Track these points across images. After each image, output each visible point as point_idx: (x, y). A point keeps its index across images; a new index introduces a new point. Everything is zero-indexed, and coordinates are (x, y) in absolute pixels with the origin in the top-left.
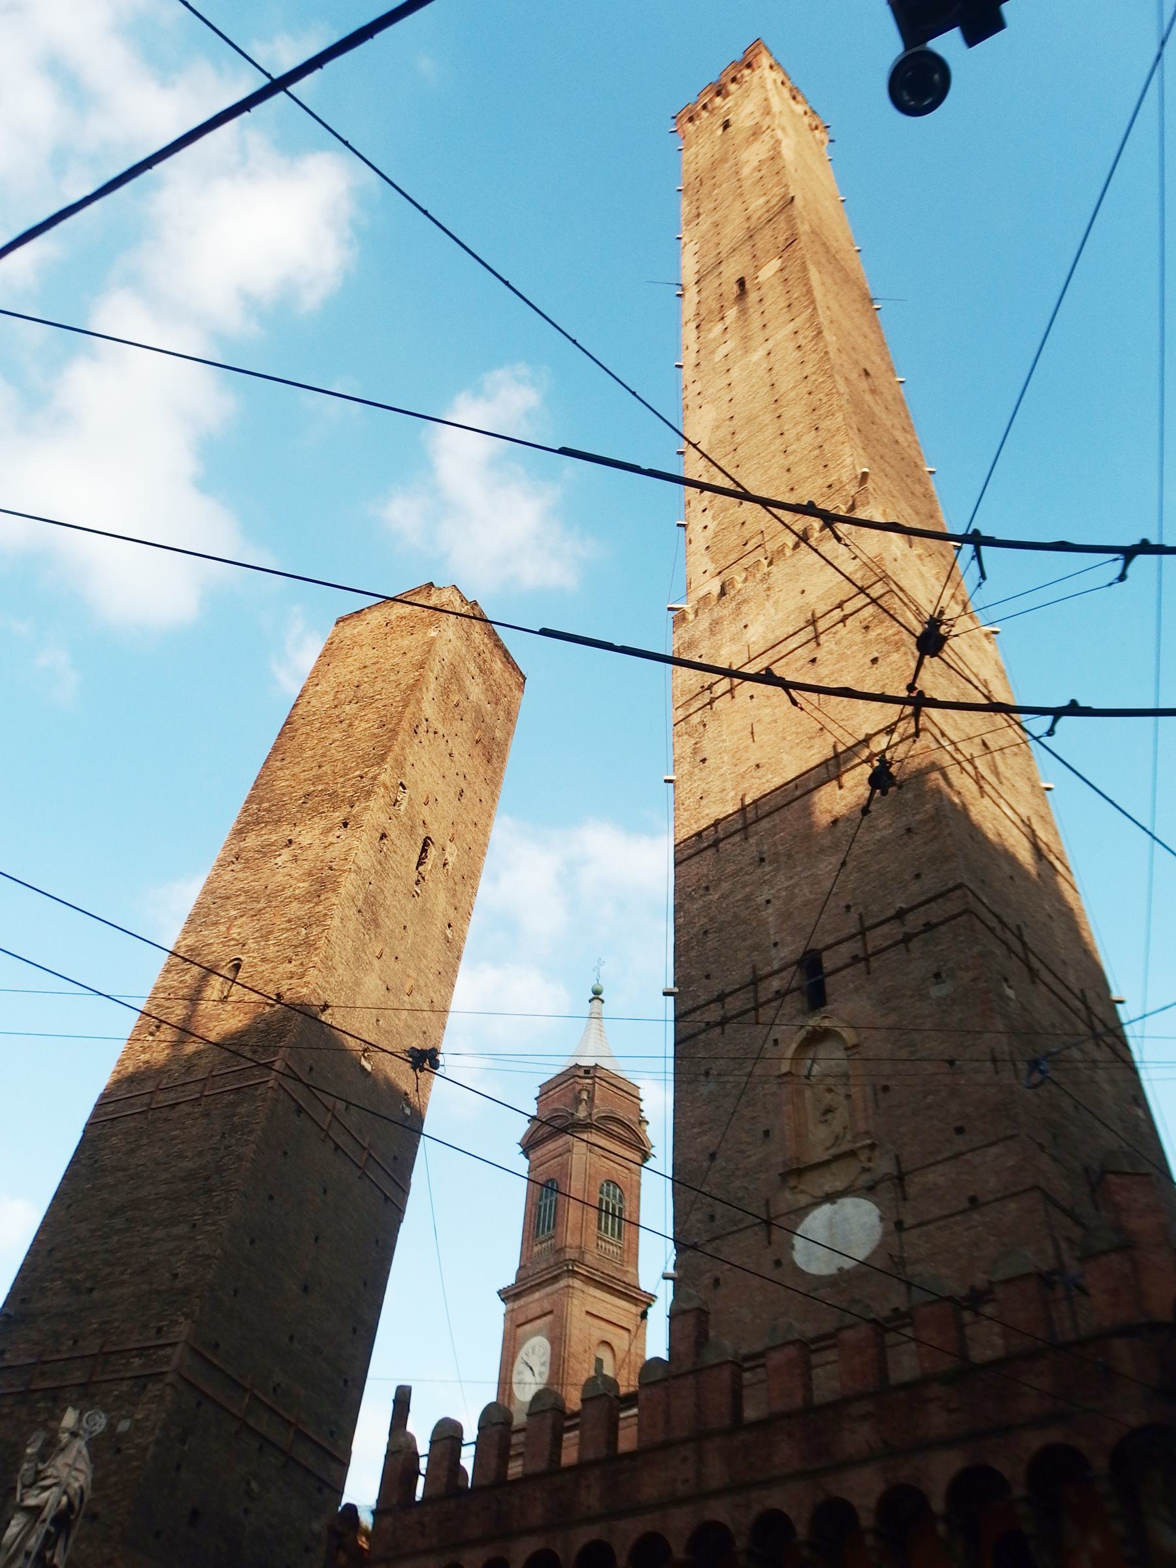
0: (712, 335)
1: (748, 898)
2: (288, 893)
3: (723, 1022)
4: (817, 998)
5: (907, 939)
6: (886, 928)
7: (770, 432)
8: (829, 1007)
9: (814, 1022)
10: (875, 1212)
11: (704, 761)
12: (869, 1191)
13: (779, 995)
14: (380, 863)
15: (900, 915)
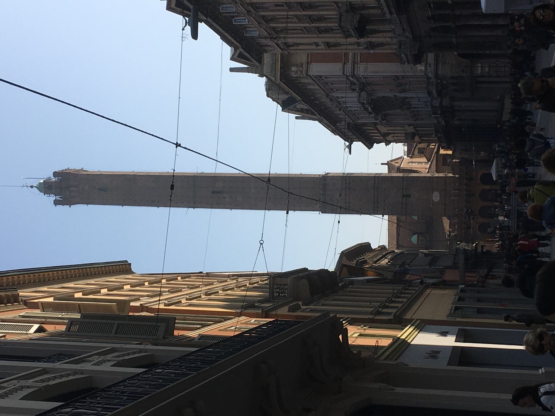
4: (409, 196)
12: (433, 193)
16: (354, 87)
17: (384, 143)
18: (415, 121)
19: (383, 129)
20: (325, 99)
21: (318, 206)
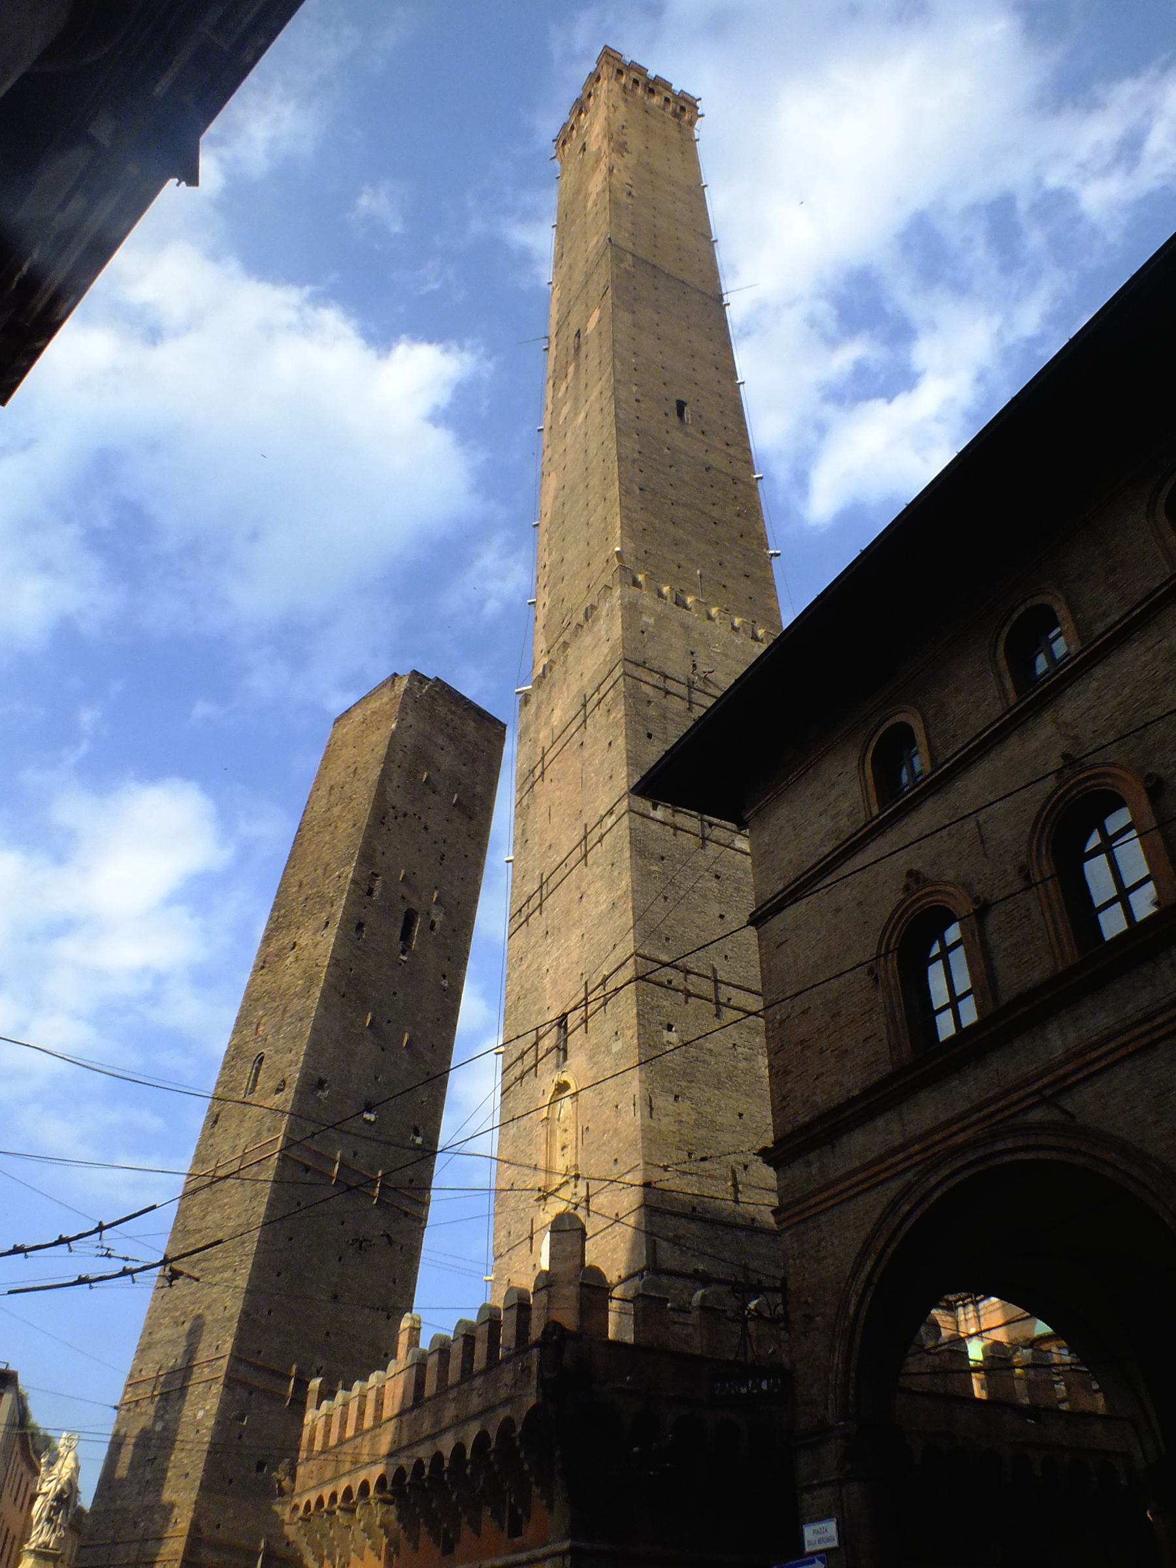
0: (560, 395)
1: (538, 969)
2: (292, 991)
7: (582, 502)
8: (567, 1063)
13: (548, 1052)
14: (359, 948)
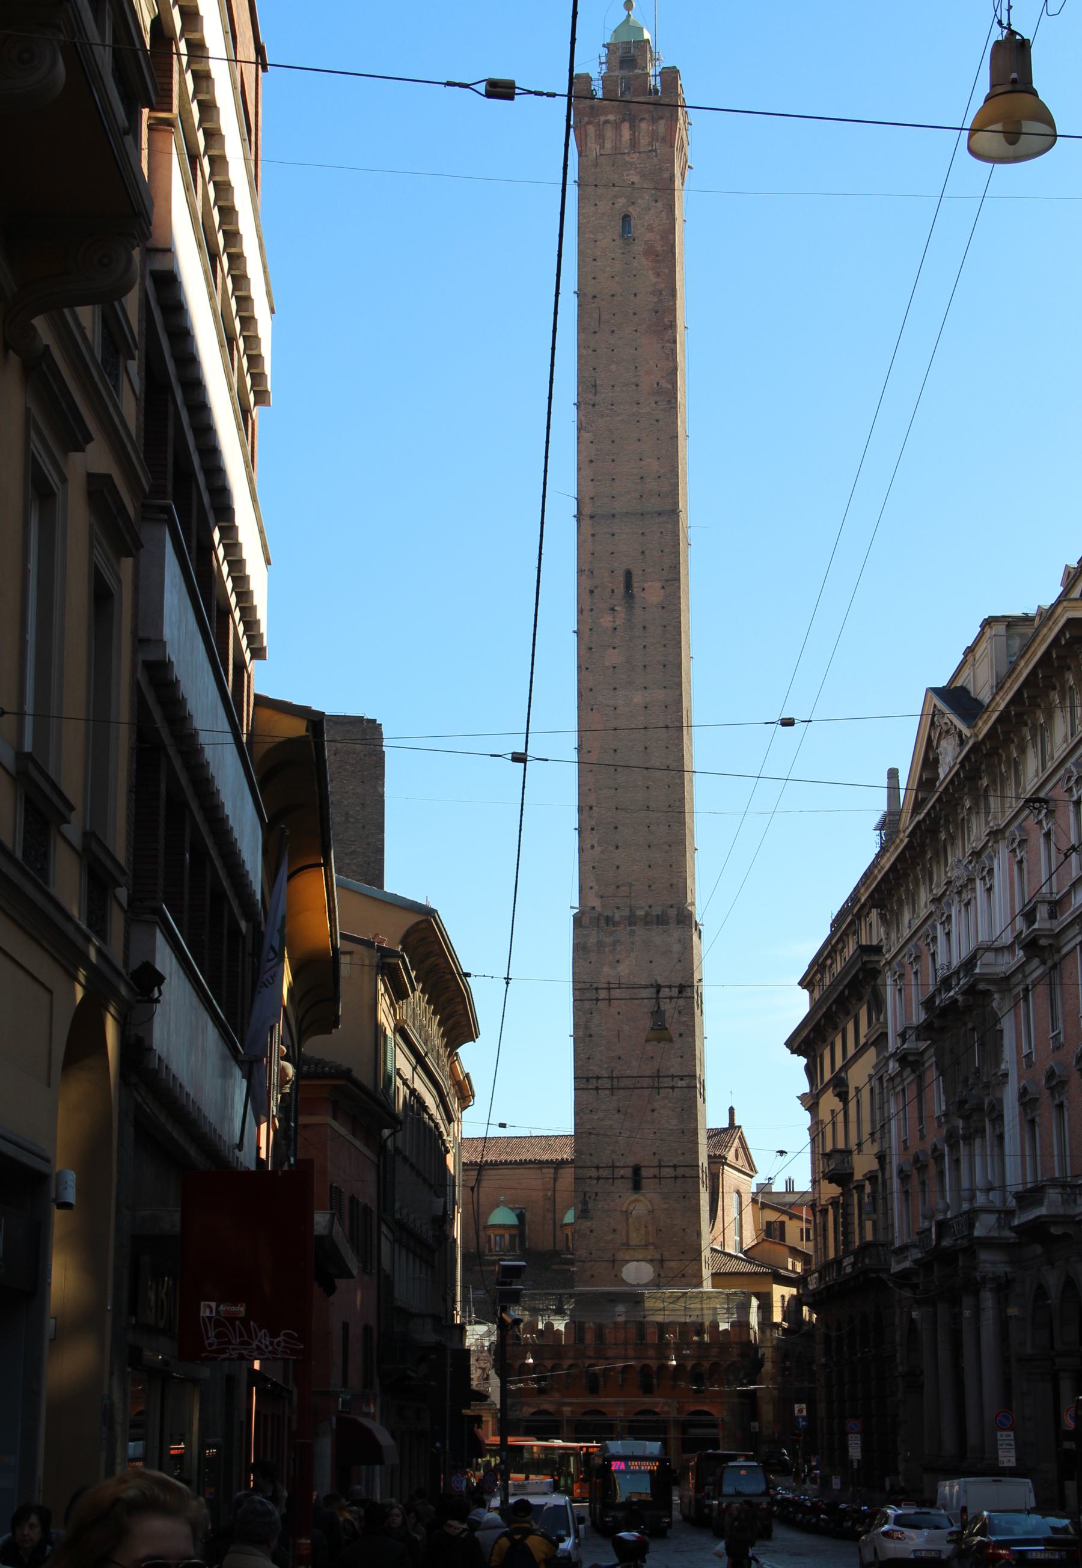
3: (598, 1178)
4: (637, 1186)
5: (676, 1178)
6: (668, 1170)
9: (636, 1196)
10: (652, 1270)
11: (591, 1036)
13: (622, 1177)
15: (675, 1167)
16: (1043, 911)
17: (807, 1090)
18: (901, 1171)
19: (859, 1075)
20: (977, 832)
21: (596, 903)
